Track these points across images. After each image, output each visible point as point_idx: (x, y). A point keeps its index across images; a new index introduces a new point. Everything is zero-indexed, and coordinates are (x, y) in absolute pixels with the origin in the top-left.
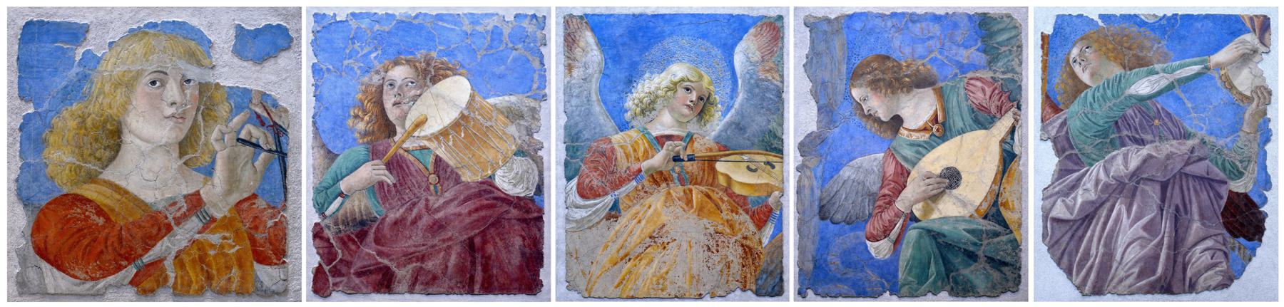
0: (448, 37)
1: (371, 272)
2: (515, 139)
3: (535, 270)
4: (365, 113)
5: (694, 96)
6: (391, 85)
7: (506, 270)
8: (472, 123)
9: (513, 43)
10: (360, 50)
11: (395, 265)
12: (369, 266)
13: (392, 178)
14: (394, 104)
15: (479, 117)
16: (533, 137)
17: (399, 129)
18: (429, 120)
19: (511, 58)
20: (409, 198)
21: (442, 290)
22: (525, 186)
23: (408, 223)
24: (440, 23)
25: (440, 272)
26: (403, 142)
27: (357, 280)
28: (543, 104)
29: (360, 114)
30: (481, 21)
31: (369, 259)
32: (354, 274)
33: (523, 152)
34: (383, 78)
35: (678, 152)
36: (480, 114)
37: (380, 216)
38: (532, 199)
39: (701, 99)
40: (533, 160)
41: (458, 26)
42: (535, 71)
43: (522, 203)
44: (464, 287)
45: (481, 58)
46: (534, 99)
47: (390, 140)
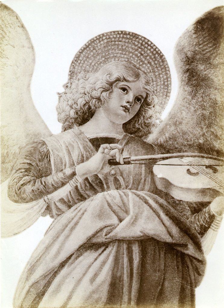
5: (130, 97)
35: (114, 157)
39: (137, 99)
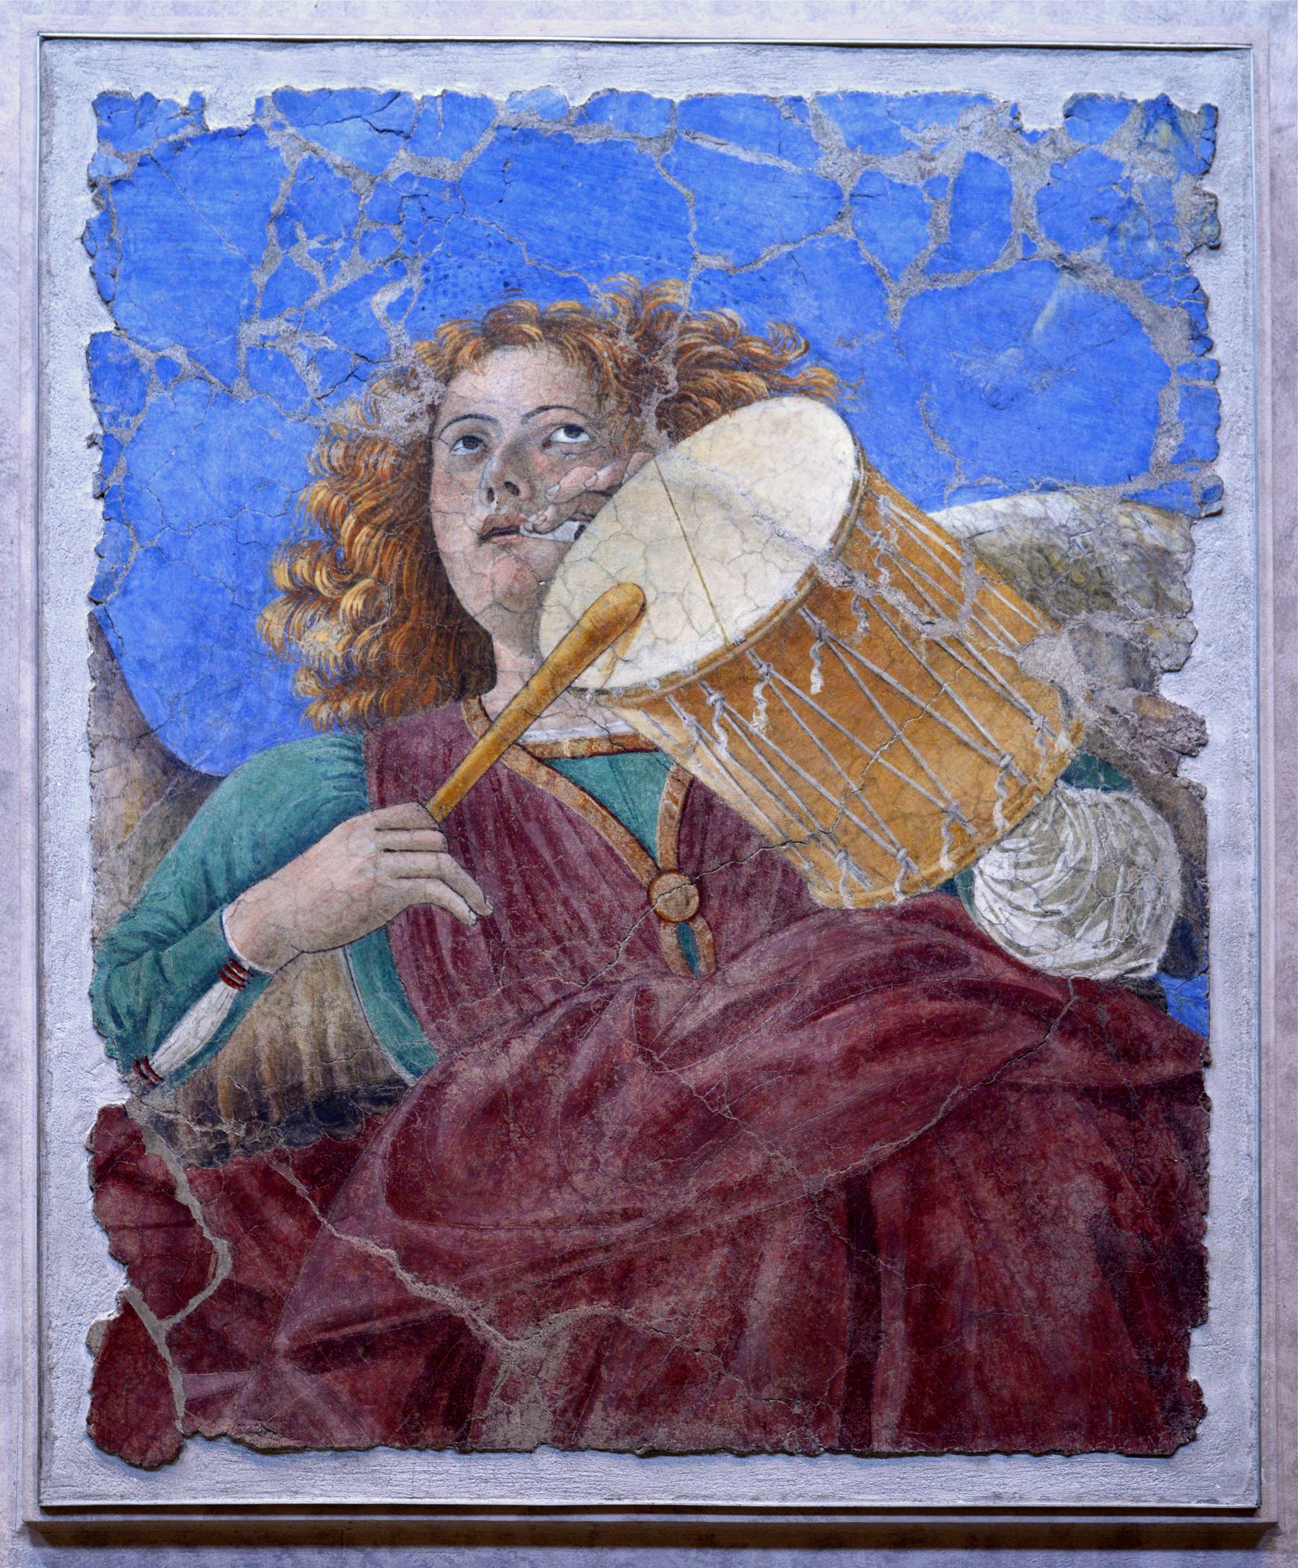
0: (743, 208)
1: (373, 1346)
2: (1067, 702)
3: (1168, 1338)
4: (345, 574)
6: (470, 440)
7: (1027, 1335)
8: (863, 624)
9: (1059, 237)
10: (319, 274)
11: (490, 1309)
13: (474, 889)
14: (488, 534)
15: (896, 598)
16: (1155, 696)
17: (507, 656)
18: (652, 611)
19: (1050, 309)
20: (556, 986)
21: (717, 1433)
23: (554, 1111)
24: (707, 143)
25: (706, 1344)
26: (530, 715)
27: (305, 1386)
28: (1201, 532)
29: (321, 580)
30: (906, 134)
31: (365, 1281)
32: (293, 1355)
33: (1106, 765)
34: (433, 409)
37: (417, 1073)
38: (1150, 995)
40: (1159, 806)
41: (795, 160)
42: (1167, 372)
43: (1103, 1014)
44: (822, 1416)
45: (906, 312)
46: (1159, 508)
47: (466, 709)
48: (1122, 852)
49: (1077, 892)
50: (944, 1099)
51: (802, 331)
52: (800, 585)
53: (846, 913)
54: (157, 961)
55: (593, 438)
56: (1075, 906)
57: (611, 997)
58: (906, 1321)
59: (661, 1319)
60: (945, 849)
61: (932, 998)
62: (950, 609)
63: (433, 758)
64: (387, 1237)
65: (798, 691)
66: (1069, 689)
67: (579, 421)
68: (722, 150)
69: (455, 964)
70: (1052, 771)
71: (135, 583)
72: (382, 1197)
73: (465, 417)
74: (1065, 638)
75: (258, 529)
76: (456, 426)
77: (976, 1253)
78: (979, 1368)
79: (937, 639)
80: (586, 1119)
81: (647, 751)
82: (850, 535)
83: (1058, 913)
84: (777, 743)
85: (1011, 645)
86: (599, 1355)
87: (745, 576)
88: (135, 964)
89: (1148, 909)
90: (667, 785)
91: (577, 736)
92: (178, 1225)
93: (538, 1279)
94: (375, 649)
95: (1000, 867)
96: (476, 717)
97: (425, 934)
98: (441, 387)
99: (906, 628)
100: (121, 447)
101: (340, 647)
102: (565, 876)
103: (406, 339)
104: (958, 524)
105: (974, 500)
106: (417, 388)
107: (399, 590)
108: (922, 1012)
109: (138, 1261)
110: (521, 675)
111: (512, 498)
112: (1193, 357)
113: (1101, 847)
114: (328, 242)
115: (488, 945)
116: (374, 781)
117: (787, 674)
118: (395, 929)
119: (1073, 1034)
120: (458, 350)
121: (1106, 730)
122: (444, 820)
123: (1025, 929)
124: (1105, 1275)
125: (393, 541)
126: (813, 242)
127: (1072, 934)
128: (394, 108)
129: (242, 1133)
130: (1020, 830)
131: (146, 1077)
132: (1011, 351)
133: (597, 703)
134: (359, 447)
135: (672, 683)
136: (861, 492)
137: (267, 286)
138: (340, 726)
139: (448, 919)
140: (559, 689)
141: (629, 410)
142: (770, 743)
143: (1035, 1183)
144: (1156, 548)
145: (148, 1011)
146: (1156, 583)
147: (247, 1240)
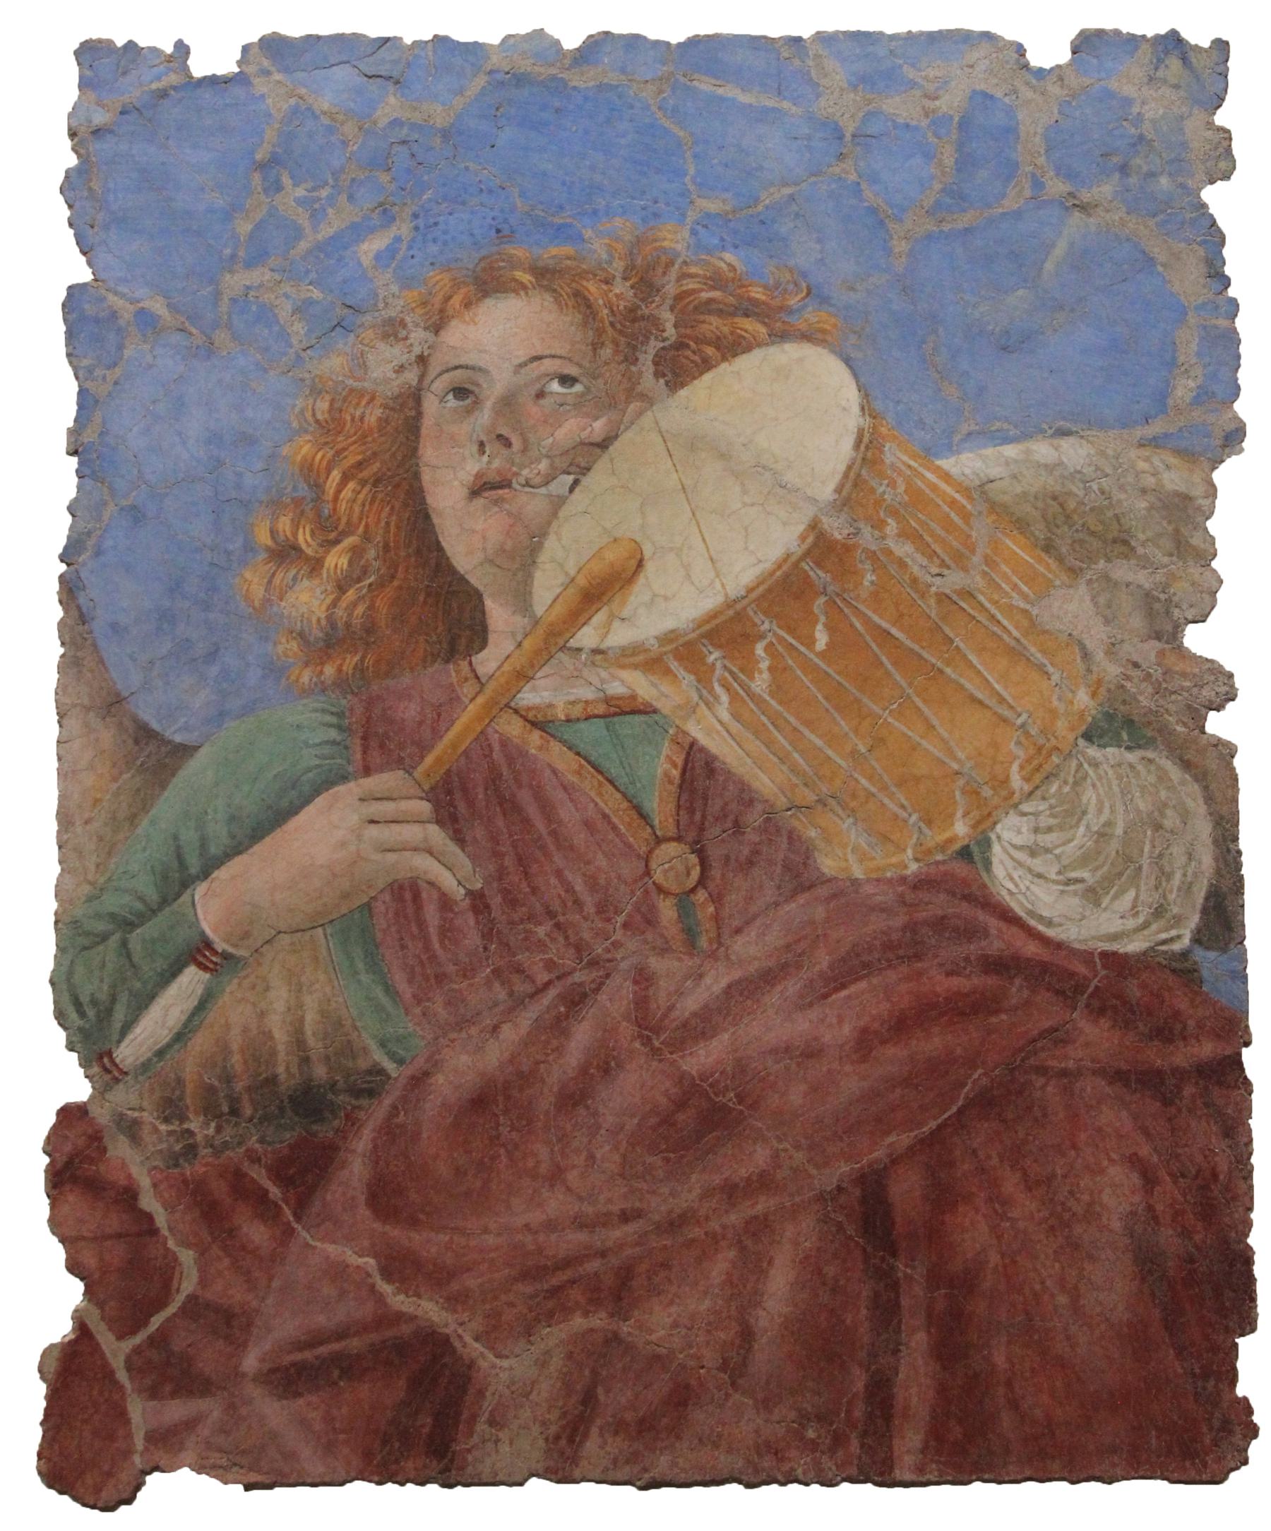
1: (350, 1367)
2: (1086, 655)
3: (1215, 1349)
4: (330, 532)
6: (460, 392)
8: (869, 577)
9: (1068, 174)
10: (304, 220)
11: (477, 1325)
12: (341, 1334)
14: (481, 487)
15: (903, 549)
17: (498, 614)
18: (650, 567)
19: (1060, 250)
20: (550, 965)
21: (724, 1461)
22: (1148, 897)
23: (546, 1102)
24: (705, 85)
25: (711, 1358)
26: (523, 676)
29: (304, 538)
30: (910, 73)
31: (343, 1293)
33: (1129, 723)
34: (422, 360)
36: (906, 534)
37: (400, 1062)
40: (1186, 765)
43: (1133, 990)
44: (838, 1440)
46: (1178, 452)
47: (454, 672)
48: (1150, 814)
49: (1101, 859)
50: (963, 1085)
51: (804, 275)
52: (803, 538)
53: (855, 882)
54: (124, 943)
55: (588, 389)
56: (1099, 873)
57: (608, 976)
58: (929, 1332)
59: (663, 1332)
60: (959, 813)
61: (949, 974)
62: (960, 561)
63: (420, 723)
64: (366, 1243)
65: (802, 649)
66: (1087, 643)
67: (572, 370)
68: (720, 91)
69: (441, 942)
70: (1072, 729)
71: (109, 543)
72: (362, 1199)
73: (456, 368)
74: (1083, 588)
75: (238, 486)
76: (446, 376)
77: (1003, 1255)
78: (1009, 1384)
79: (948, 591)
80: (582, 1111)
81: (646, 713)
82: (855, 485)
83: (1082, 881)
84: (780, 703)
85: (1025, 597)
86: (594, 1372)
87: (746, 529)
88: (101, 948)
89: (1178, 876)
90: (666, 747)
91: (572, 698)
92: (139, 1235)
93: (529, 1290)
94: (360, 609)
95: (1019, 832)
96: (466, 680)
97: (410, 910)
98: (430, 336)
99: (914, 581)
100: (97, 402)
101: (324, 607)
102: (559, 847)
103: (394, 288)
104: (967, 471)
105: (985, 446)
106: (406, 338)
107: (386, 548)
108: (938, 989)
109: (96, 1276)
110: (513, 634)
111: (505, 452)
112: (1211, 296)
113: (1126, 811)
114: (314, 189)
115: (477, 923)
116: (358, 749)
117: (790, 630)
118: (379, 907)
119: (1102, 1011)
120: (448, 299)
121: (1128, 685)
122: (432, 789)
123: (1048, 899)
124: (1143, 1279)
125: (380, 496)
126: (815, 183)
127: (1097, 904)
128: (383, 53)
129: (211, 1131)
130: (1038, 793)
131: (107, 1071)
132: (1020, 292)
133: (593, 663)
134: (345, 400)
135: (671, 641)
136: (866, 440)
137: (251, 236)
138: (323, 691)
139: (435, 895)
140: (553, 650)
141: (626, 360)
142: (773, 702)
143: (1065, 1177)
144: (1177, 494)
145: (113, 999)
146: (1177, 531)
147: (216, 1250)
